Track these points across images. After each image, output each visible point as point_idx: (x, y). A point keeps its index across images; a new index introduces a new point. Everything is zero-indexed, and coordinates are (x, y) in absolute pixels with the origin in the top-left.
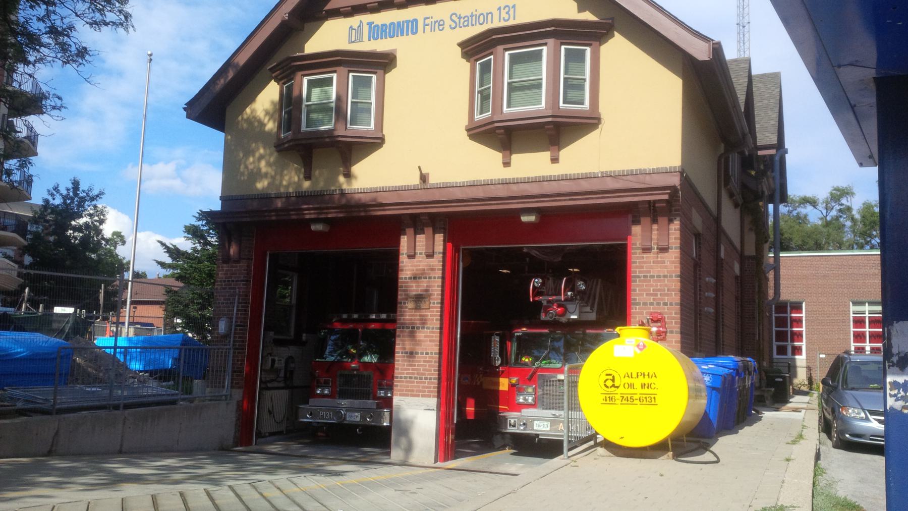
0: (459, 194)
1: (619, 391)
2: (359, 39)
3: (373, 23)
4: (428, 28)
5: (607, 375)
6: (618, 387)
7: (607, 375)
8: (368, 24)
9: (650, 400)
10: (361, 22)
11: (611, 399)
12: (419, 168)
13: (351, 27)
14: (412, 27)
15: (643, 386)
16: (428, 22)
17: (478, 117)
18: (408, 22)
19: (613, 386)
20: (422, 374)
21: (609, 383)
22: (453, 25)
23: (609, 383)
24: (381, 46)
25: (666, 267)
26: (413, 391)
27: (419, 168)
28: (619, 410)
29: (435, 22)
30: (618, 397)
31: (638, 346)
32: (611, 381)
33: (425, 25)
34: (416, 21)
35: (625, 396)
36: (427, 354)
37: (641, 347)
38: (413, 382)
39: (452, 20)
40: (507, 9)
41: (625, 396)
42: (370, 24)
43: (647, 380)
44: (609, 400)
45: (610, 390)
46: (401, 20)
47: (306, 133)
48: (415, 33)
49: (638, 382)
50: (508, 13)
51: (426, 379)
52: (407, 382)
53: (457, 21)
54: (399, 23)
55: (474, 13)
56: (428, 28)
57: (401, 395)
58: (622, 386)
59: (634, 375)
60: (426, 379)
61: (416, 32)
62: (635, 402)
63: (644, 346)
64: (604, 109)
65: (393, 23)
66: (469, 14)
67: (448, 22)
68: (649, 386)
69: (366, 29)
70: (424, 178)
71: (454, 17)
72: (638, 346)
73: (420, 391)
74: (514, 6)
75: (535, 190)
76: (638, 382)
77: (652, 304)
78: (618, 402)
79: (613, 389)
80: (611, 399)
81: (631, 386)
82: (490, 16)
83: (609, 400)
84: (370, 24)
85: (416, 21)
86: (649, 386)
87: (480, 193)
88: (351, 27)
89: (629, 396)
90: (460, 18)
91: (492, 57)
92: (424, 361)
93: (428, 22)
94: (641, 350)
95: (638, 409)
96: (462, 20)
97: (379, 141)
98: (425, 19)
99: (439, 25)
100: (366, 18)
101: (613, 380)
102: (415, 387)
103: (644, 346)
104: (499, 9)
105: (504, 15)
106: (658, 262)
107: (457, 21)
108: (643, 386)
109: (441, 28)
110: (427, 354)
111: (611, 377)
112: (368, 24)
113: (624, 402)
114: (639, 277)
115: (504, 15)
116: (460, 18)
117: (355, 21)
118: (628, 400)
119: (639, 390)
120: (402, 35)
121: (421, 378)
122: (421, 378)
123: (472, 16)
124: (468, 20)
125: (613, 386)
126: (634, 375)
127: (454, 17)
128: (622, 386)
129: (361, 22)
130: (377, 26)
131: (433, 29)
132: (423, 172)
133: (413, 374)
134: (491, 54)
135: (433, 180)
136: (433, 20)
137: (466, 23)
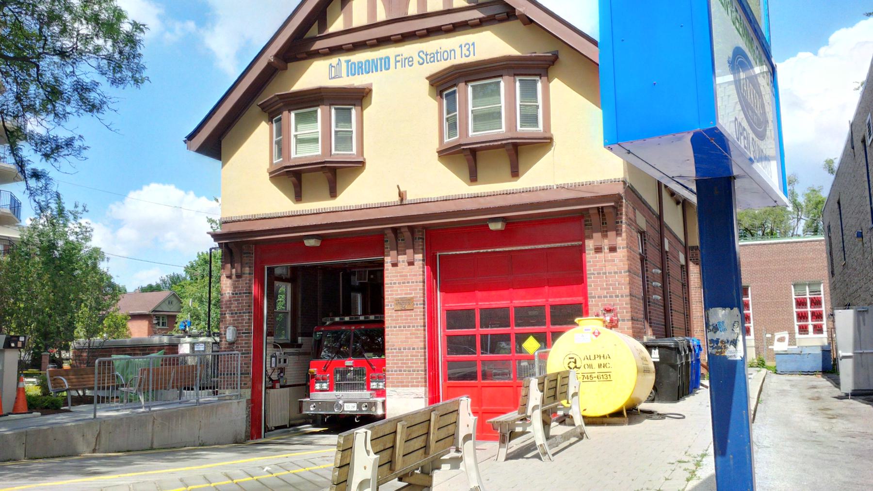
9: (606, 377)
12: (398, 187)
14: (386, 63)
15: (600, 366)
16: (398, 58)
17: (446, 140)
18: (381, 59)
19: (576, 367)
22: (421, 61)
24: (358, 81)
25: (615, 265)
27: (398, 187)
33: (397, 62)
36: (414, 349)
42: (348, 62)
43: (602, 361)
49: (595, 363)
50: (468, 50)
53: (424, 56)
54: (373, 60)
58: (582, 367)
59: (592, 358)
60: (414, 371)
63: (599, 333)
64: (555, 131)
66: (435, 52)
67: (416, 59)
69: (344, 65)
71: (421, 54)
73: (409, 382)
74: (473, 44)
76: (595, 363)
77: (606, 297)
81: (590, 366)
85: (388, 58)
93: (398, 58)
96: (429, 57)
100: (344, 58)
101: (575, 362)
103: (599, 333)
104: (461, 46)
106: (609, 261)
107: (424, 56)
108: (600, 366)
110: (414, 349)
114: (593, 274)
116: (427, 55)
117: (334, 60)
123: (437, 53)
125: (576, 367)
126: (592, 358)
127: (421, 54)
128: (582, 367)
130: (354, 63)
131: (404, 66)
135: (410, 197)
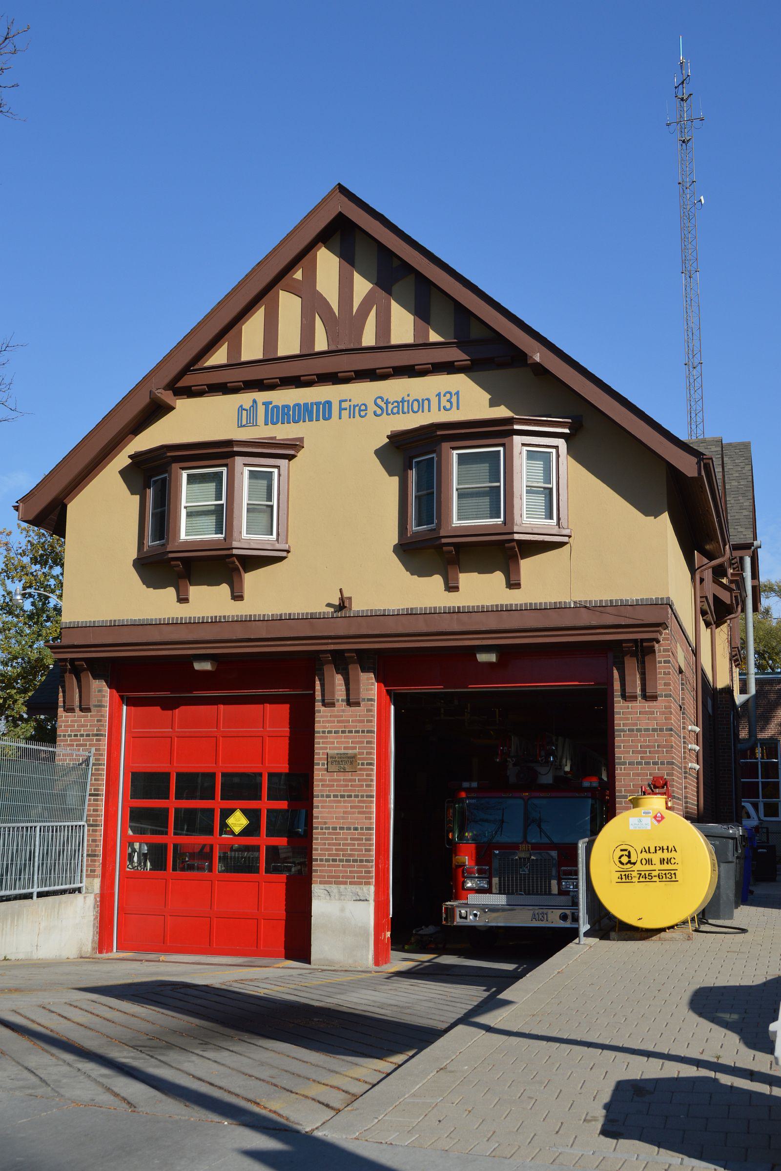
0: (393, 627)
1: (635, 868)
2: (252, 422)
3: (271, 403)
4: (345, 414)
5: (622, 850)
6: (634, 864)
7: (622, 850)
8: (263, 404)
9: (670, 877)
10: (255, 401)
11: (627, 877)
12: (341, 590)
13: (241, 406)
14: (325, 410)
15: (662, 861)
16: (344, 405)
17: (413, 527)
18: (318, 404)
19: (629, 862)
20: (350, 855)
21: (625, 860)
22: (379, 411)
23: (625, 860)
24: (283, 432)
25: (655, 719)
26: (338, 877)
27: (341, 590)
28: (637, 889)
29: (355, 406)
30: (635, 874)
31: (655, 817)
32: (626, 857)
33: (341, 409)
34: (329, 403)
35: (643, 873)
36: (356, 829)
37: (659, 818)
38: (338, 866)
39: (376, 404)
40: (448, 396)
41: (643, 873)
42: (266, 404)
43: (666, 855)
44: (625, 878)
45: (625, 867)
46: (309, 400)
47: (186, 543)
48: (328, 417)
49: (656, 858)
50: (449, 401)
51: (355, 861)
52: (329, 866)
53: (384, 406)
54: (306, 405)
55: (406, 398)
56: (345, 414)
57: (321, 883)
58: (639, 862)
59: (652, 850)
60: (355, 861)
61: (330, 417)
62: (654, 879)
63: (662, 818)
65: (298, 405)
66: (400, 400)
67: (372, 408)
68: (669, 861)
69: (261, 410)
70: (342, 606)
71: (379, 401)
72: (655, 817)
73: (347, 877)
74: (457, 393)
75: (492, 623)
76: (656, 858)
77: (639, 763)
78: (635, 880)
79: (629, 865)
80: (627, 877)
81: (649, 862)
82: (426, 402)
83: (625, 878)
84: (266, 404)
85: (329, 403)
86: (669, 861)
87: (421, 626)
88: (241, 406)
89: (647, 873)
90: (387, 403)
91: (434, 455)
92: (352, 839)
93: (344, 405)
94: (659, 821)
95: (657, 888)
96: (390, 406)
97: (284, 554)
98: (341, 402)
99: (360, 411)
100: (262, 397)
101: (629, 856)
102: (341, 871)
103: (662, 818)
104: (439, 395)
105: (444, 402)
106: (646, 713)
107: (384, 406)
108: (662, 861)
109: (363, 413)
110: (356, 829)
111: (626, 853)
112: (263, 404)
113: (641, 879)
114: (623, 731)
115: (444, 402)
116: (387, 403)
117: (245, 399)
118: (646, 877)
119: (659, 866)
120: (311, 420)
121: (347, 861)
122: (347, 861)
123: (403, 401)
124: (398, 407)
125: (629, 862)
126: (652, 850)
127: (379, 401)
128: (639, 862)
129: (255, 401)
130: (277, 407)
131: (352, 415)
132: (346, 595)
133: (338, 855)
134: (433, 452)
135: (358, 606)
136: (352, 404)
137: (395, 410)
